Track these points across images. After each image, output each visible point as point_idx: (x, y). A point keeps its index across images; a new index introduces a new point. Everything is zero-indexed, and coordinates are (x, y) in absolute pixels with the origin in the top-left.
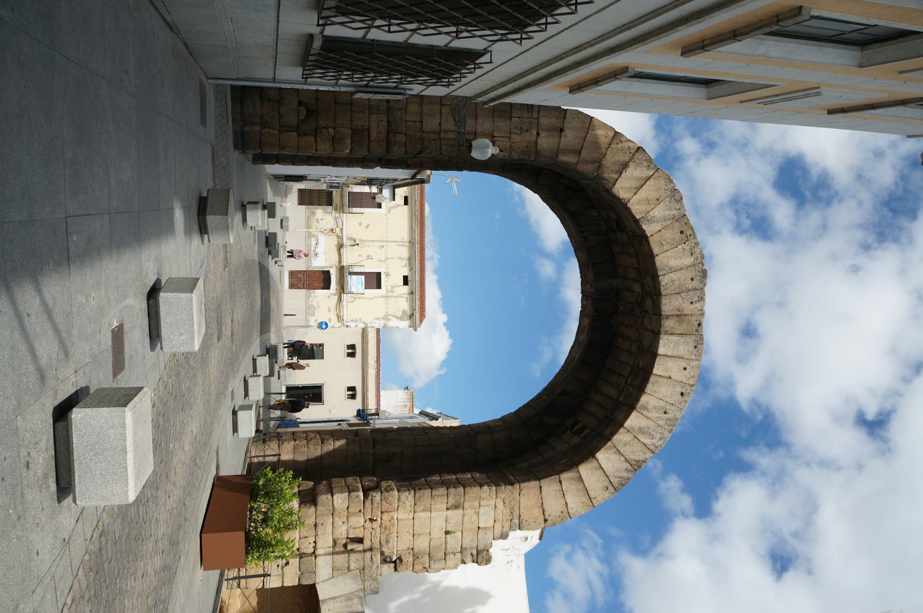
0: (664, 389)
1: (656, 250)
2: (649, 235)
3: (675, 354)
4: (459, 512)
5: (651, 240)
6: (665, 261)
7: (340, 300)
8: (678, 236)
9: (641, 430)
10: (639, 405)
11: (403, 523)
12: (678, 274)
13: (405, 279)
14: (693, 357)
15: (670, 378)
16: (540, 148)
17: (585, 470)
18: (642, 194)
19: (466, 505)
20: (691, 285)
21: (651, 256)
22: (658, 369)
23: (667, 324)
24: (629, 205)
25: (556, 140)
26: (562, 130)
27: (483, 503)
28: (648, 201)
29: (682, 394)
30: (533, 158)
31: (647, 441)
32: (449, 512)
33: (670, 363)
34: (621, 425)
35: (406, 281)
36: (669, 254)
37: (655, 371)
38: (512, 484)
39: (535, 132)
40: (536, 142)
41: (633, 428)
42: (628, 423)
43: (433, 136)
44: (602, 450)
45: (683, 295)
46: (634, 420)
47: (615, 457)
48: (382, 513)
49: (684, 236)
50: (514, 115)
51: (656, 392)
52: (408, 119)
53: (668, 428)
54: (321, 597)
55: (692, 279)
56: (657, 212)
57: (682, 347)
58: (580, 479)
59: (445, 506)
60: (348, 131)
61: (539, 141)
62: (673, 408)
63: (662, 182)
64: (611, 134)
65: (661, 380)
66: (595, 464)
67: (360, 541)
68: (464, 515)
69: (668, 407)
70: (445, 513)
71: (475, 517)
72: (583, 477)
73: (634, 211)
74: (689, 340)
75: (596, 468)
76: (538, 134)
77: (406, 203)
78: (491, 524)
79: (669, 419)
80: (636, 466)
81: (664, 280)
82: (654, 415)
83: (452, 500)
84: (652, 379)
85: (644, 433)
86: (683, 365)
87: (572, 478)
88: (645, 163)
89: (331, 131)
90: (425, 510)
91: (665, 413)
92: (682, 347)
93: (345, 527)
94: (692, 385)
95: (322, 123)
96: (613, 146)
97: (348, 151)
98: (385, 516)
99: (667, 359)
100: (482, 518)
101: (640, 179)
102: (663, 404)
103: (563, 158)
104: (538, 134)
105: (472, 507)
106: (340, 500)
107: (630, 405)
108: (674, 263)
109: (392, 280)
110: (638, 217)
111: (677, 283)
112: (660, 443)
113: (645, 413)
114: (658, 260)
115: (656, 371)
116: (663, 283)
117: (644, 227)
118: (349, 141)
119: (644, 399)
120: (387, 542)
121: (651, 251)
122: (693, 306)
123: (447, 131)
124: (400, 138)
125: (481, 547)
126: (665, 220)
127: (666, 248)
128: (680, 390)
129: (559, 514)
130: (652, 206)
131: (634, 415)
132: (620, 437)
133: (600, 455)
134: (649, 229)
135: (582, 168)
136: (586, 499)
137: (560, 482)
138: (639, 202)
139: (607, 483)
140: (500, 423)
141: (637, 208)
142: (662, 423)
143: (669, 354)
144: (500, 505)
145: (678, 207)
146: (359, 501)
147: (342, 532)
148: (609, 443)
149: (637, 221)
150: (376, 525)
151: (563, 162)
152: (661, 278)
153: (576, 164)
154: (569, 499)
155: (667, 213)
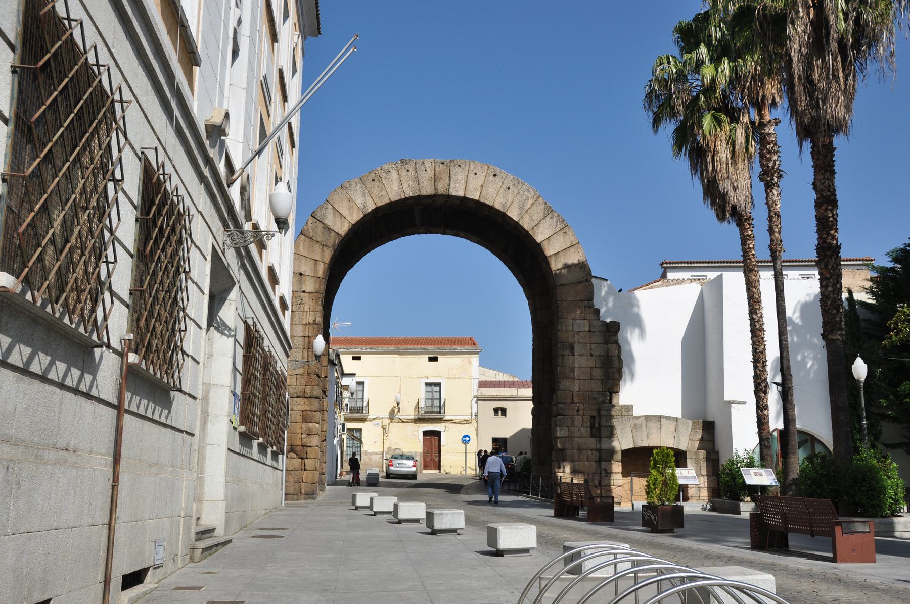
0: (491, 190)
1: (386, 201)
3: (464, 183)
4: (576, 348)
5: (379, 205)
6: (394, 193)
7: (451, 421)
8: (376, 183)
9: (521, 208)
12: (404, 182)
13: (431, 359)
14: (467, 168)
15: (482, 186)
16: (313, 291)
17: (549, 251)
18: (345, 212)
19: (571, 341)
20: (412, 172)
21: (391, 204)
22: (475, 196)
23: (441, 190)
24: (353, 222)
25: (308, 278)
26: (301, 274)
27: (570, 328)
28: (350, 209)
29: (495, 175)
30: (320, 295)
31: (530, 202)
33: (471, 186)
34: (517, 223)
35: (433, 359)
36: (389, 191)
37: (477, 198)
38: (558, 307)
41: (519, 214)
42: (516, 218)
46: (514, 214)
47: (541, 227)
49: (376, 179)
54: (632, 446)
56: (359, 201)
57: (459, 177)
59: (571, 357)
60: (304, 425)
62: (505, 182)
63: (336, 197)
64: (302, 237)
65: (483, 193)
66: (545, 243)
67: (593, 417)
68: (579, 343)
69: (504, 186)
71: (581, 334)
75: (549, 242)
76: (304, 292)
77: (359, 358)
78: (586, 322)
80: (549, 211)
81: (409, 193)
82: (510, 198)
83: (568, 352)
84: (482, 200)
85: (524, 205)
86: (472, 175)
87: (556, 260)
88: (323, 211)
89: (304, 436)
90: (573, 371)
92: (459, 177)
95: (299, 443)
96: (311, 235)
98: (576, 400)
100: (582, 329)
102: (502, 190)
103: (320, 274)
104: (304, 292)
105: (573, 337)
106: (560, 432)
107: (503, 215)
108: (396, 187)
109: (433, 371)
111: (411, 183)
112: (532, 192)
113: (508, 205)
114: (394, 198)
116: (411, 194)
117: (370, 210)
118: (311, 424)
119: (498, 206)
122: (428, 169)
123: (303, 357)
124: (308, 389)
125: (604, 329)
126: (364, 194)
127: (384, 193)
128: (492, 177)
131: (509, 214)
132: (526, 224)
133: (539, 239)
134: (371, 207)
136: (572, 249)
138: (352, 215)
139: (561, 233)
142: (516, 192)
143: (463, 187)
147: (585, 431)
149: (365, 216)
150: (582, 406)
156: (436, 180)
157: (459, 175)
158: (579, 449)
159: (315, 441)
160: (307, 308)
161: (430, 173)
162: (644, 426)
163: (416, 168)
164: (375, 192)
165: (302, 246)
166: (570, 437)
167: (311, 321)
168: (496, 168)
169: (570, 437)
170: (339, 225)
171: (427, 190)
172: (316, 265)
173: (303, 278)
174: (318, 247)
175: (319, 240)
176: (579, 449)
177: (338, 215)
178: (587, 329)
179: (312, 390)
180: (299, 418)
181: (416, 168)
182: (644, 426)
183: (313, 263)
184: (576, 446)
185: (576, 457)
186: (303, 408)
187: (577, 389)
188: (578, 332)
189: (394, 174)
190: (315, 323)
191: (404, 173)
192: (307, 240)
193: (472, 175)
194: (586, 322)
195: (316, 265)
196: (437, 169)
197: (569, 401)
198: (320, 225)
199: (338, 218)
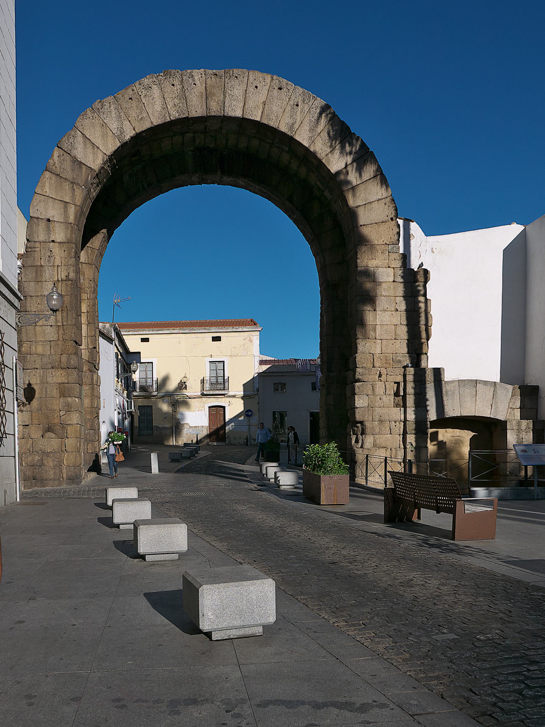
0: (275, 108)
1: (146, 125)
2: (134, 132)
3: (241, 98)
5: (138, 130)
6: (156, 114)
8: (134, 103)
10: (289, 133)
11: (384, 348)
12: (168, 100)
15: (264, 103)
18: (98, 142)
23: (215, 110)
26: (49, 220)
28: (104, 136)
32: (377, 309)
33: (250, 103)
34: (307, 149)
36: (150, 111)
37: (259, 120)
39: (52, 244)
40: (59, 243)
41: (310, 138)
42: (306, 144)
43: (61, 331)
44: (329, 168)
45: (187, 94)
50: (39, 264)
51: (277, 116)
52: (49, 353)
53: (312, 101)
55: (173, 85)
56: (114, 126)
57: (236, 92)
60: (61, 400)
61: (58, 240)
62: (292, 98)
69: (291, 103)
70: (378, 312)
73: (114, 149)
74: (230, 85)
76: (53, 241)
79: (304, 101)
81: (175, 115)
84: (265, 121)
86: (251, 89)
87: (354, 195)
91: (297, 105)
93: (384, 398)
94: (272, 79)
97: (77, 399)
98: (377, 364)
99: (246, 106)
101: (85, 145)
102: (289, 108)
103: (72, 219)
104: (53, 241)
106: (360, 402)
108: (158, 107)
110: (119, 144)
113: (296, 126)
114: (157, 121)
115: (257, 118)
117: (128, 137)
118: (69, 399)
119: (283, 128)
121: (148, 129)
122: (198, 83)
123: (57, 321)
126: (120, 117)
127: (145, 115)
128: (276, 92)
129: (387, 207)
130: (109, 130)
131: (297, 138)
134: (129, 134)
135: (79, 200)
140: (318, 258)
141: (111, 146)
143: (242, 105)
145: (108, 104)
146: (363, 385)
148: (324, 161)
150: (384, 371)
151: (76, 217)
152: (172, 118)
155: (113, 114)
156: (207, 95)
157: (236, 89)
158: (381, 421)
159: (75, 418)
160: (58, 262)
161: (200, 87)
162: (457, 392)
163: (182, 81)
164: (133, 113)
165: (47, 185)
166: (370, 407)
167: (64, 277)
168: (281, 79)
169: (370, 407)
170: (91, 156)
171: (197, 110)
173: (51, 225)
174: (67, 186)
175: (67, 177)
176: (381, 421)
177: (89, 145)
178: (392, 280)
179: (68, 359)
180: (56, 393)
181: (182, 81)
182: (457, 392)
183: (62, 205)
184: (377, 418)
185: (377, 430)
186: (60, 381)
187: (379, 351)
189: (156, 90)
190: (68, 279)
191: (168, 88)
192: (54, 177)
193: (251, 89)
196: (209, 81)
197: (370, 365)
198: (68, 158)
199: (90, 150)
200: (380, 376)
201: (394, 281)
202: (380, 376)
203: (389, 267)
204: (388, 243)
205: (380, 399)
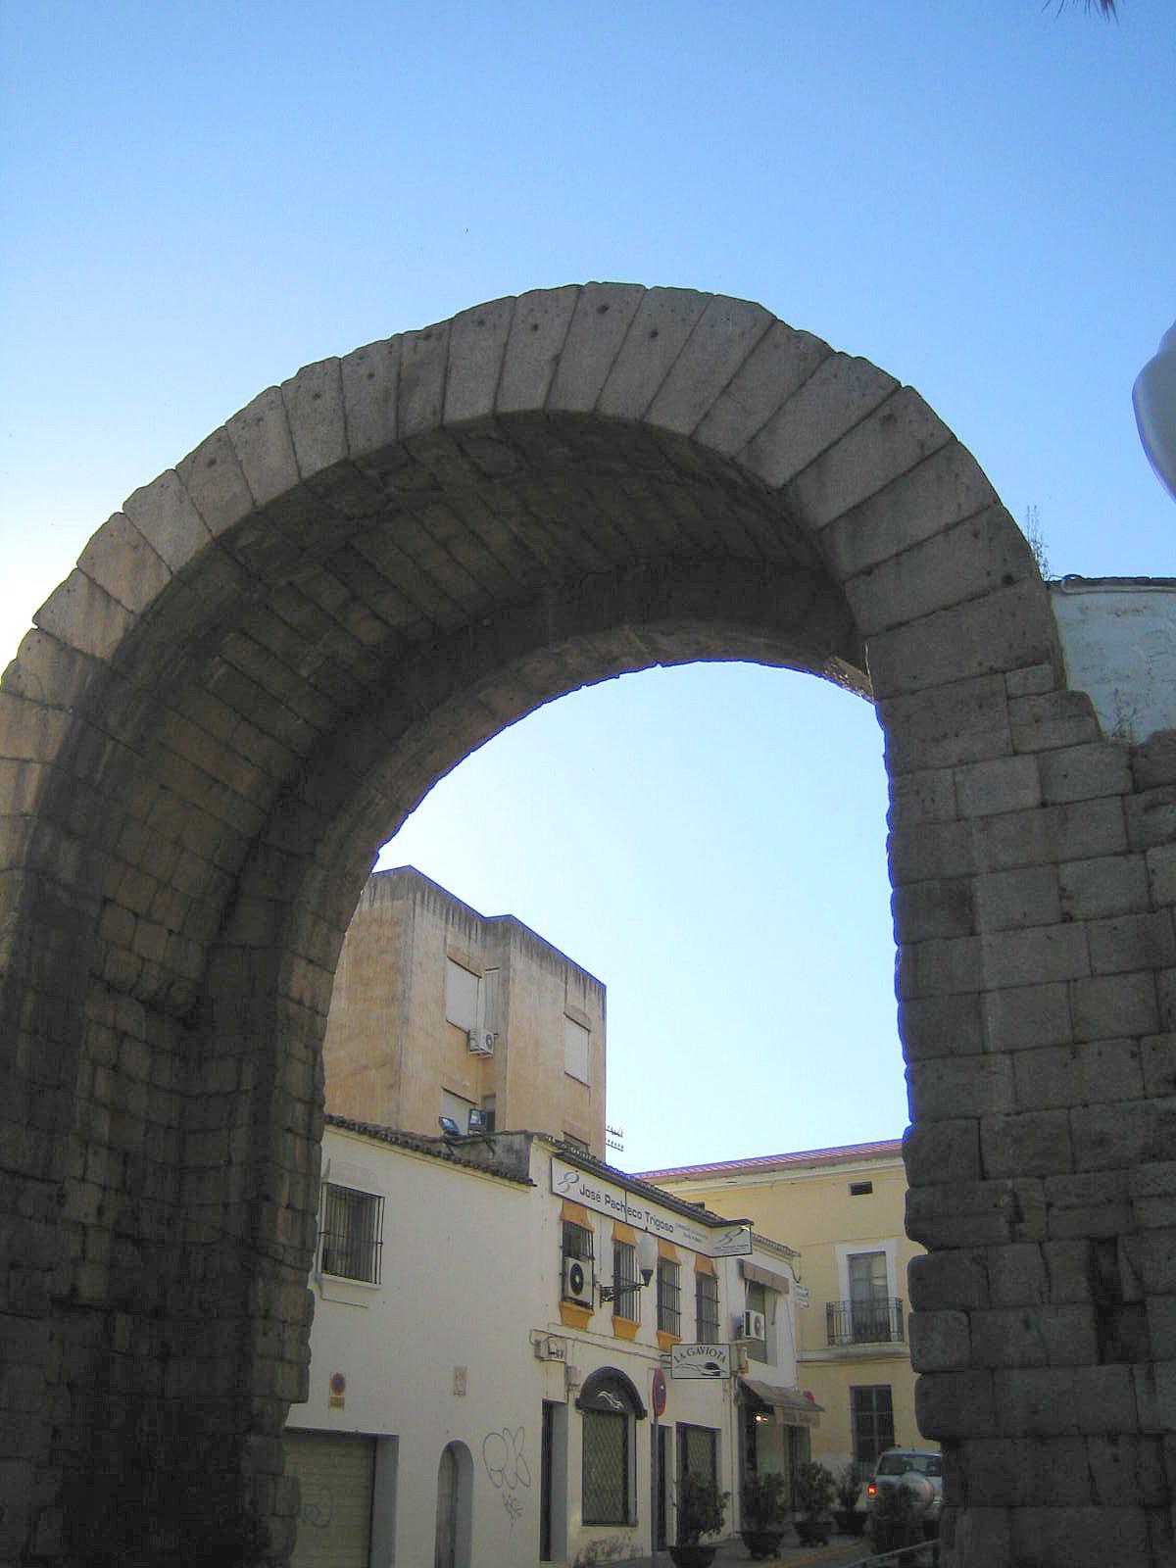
15: (557, 360)
17: (827, 506)
29: (603, 309)
31: (736, 355)
32: (982, 926)
44: (763, 473)
48: (984, 1178)
58: (856, 512)
70: (986, 938)
72: (852, 500)
98: (994, 1163)
120: (1102, 1141)
125: (1121, 780)
131: (656, 419)
137: (869, 571)
144: (955, 748)
147: (1069, 1325)
153: (44, 763)
154: (924, 525)
172: (21, 774)
178: (1030, 796)
188: (987, 820)
194: (1026, 769)
195: (21, 774)
200: (1017, 1216)
201: (1044, 805)
202: (1017, 1216)
203: (1016, 753)
204: (999, 664)
205: (1027, 1325)
